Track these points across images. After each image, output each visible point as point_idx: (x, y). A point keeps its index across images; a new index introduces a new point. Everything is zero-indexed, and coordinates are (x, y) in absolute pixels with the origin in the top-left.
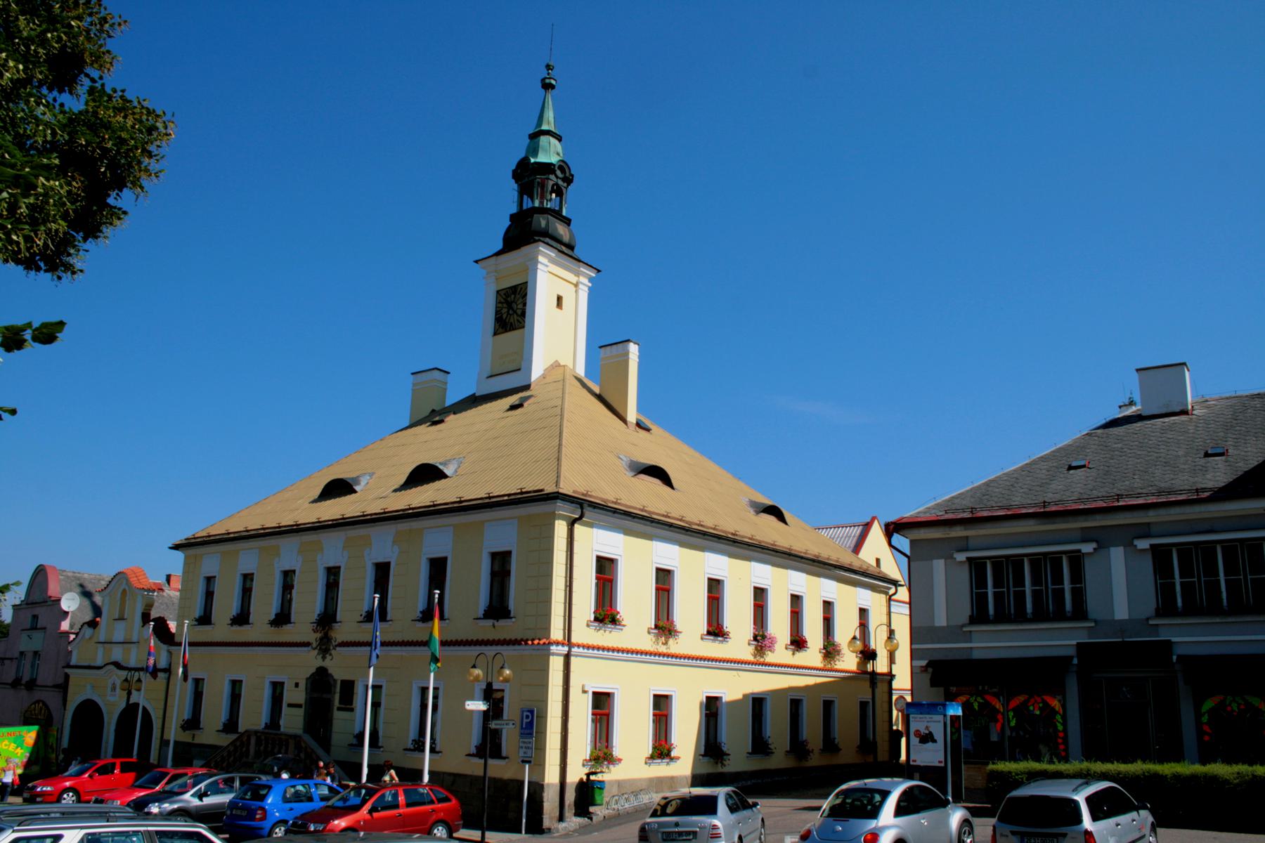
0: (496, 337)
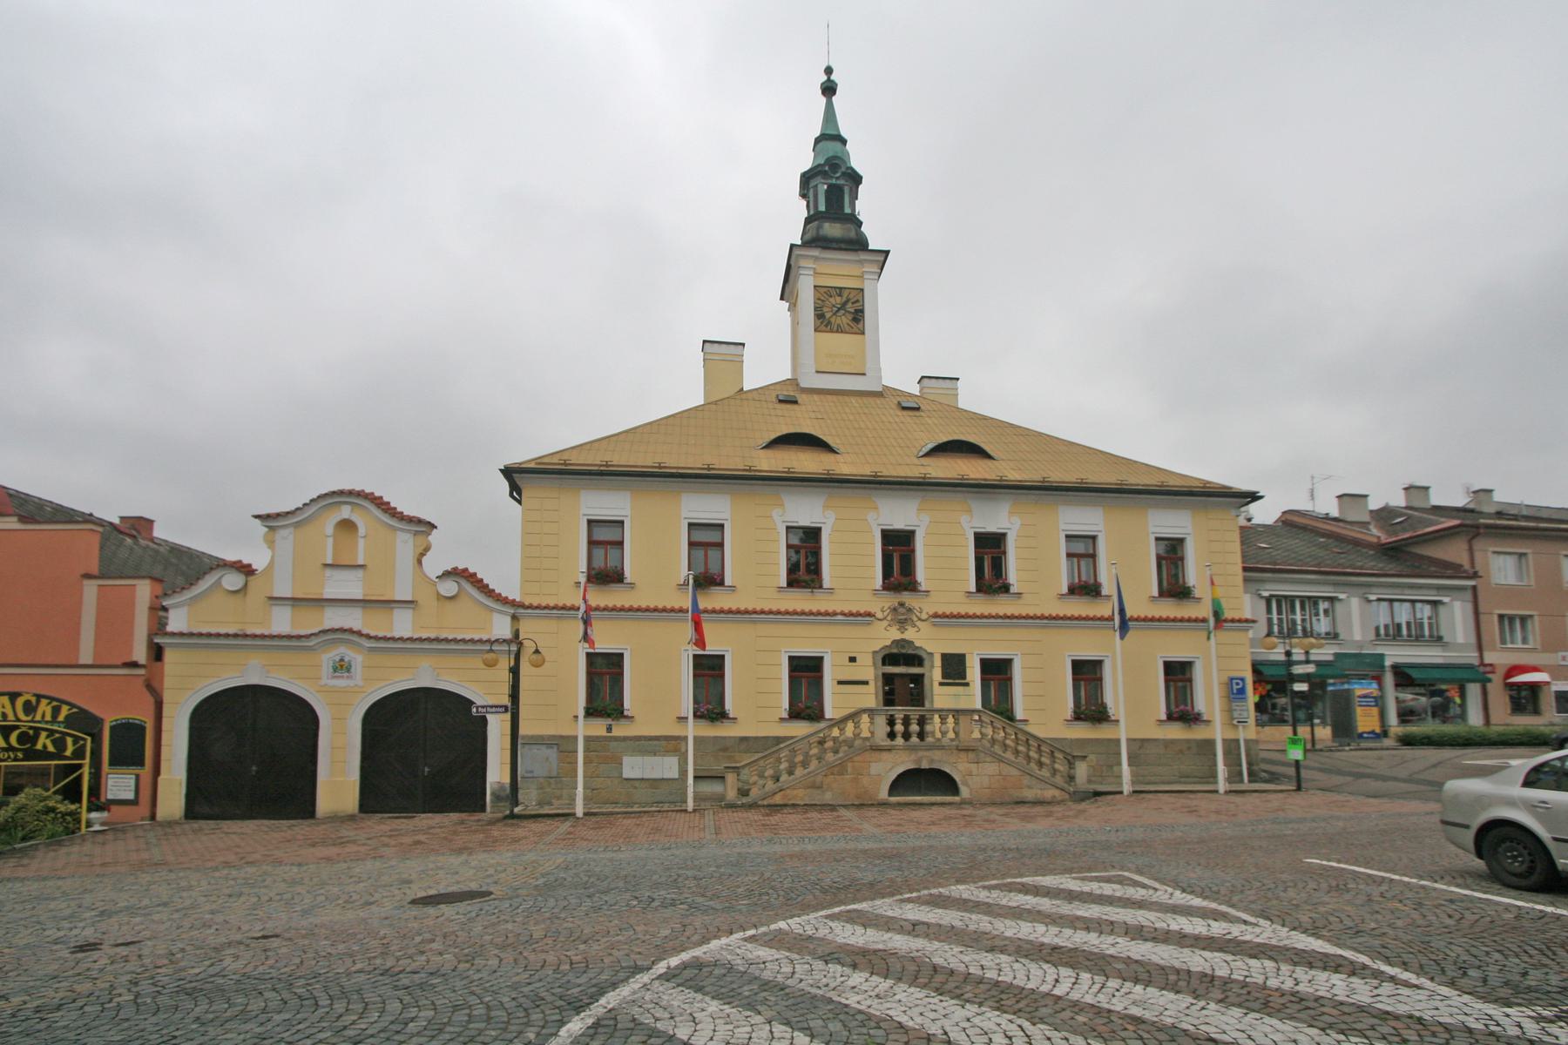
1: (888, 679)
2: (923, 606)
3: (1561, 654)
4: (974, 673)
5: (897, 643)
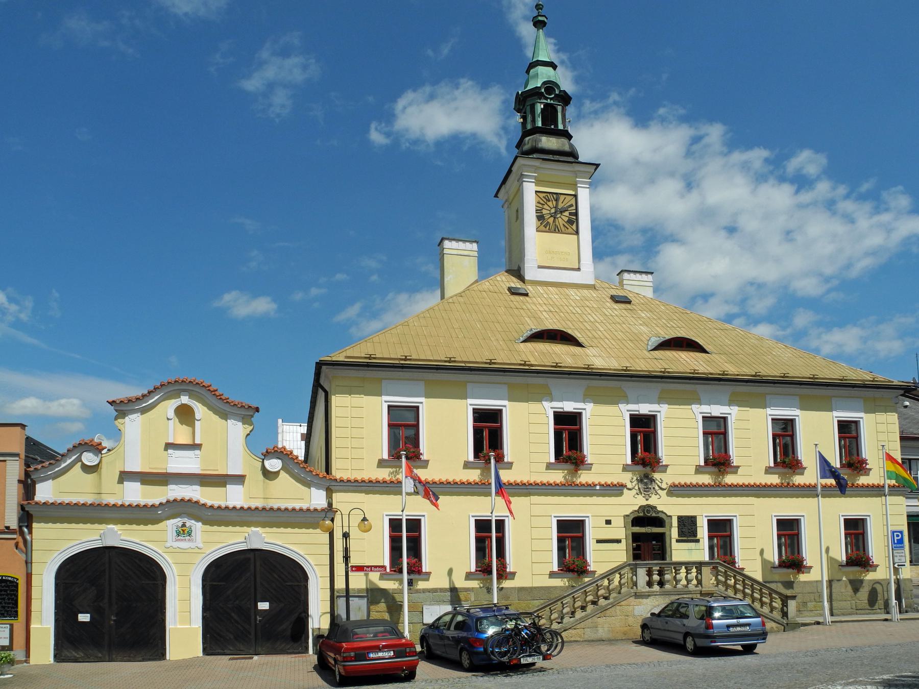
1: (636, 537)
2: (663, 479)
4: (703, 531)
5: (642, 508)
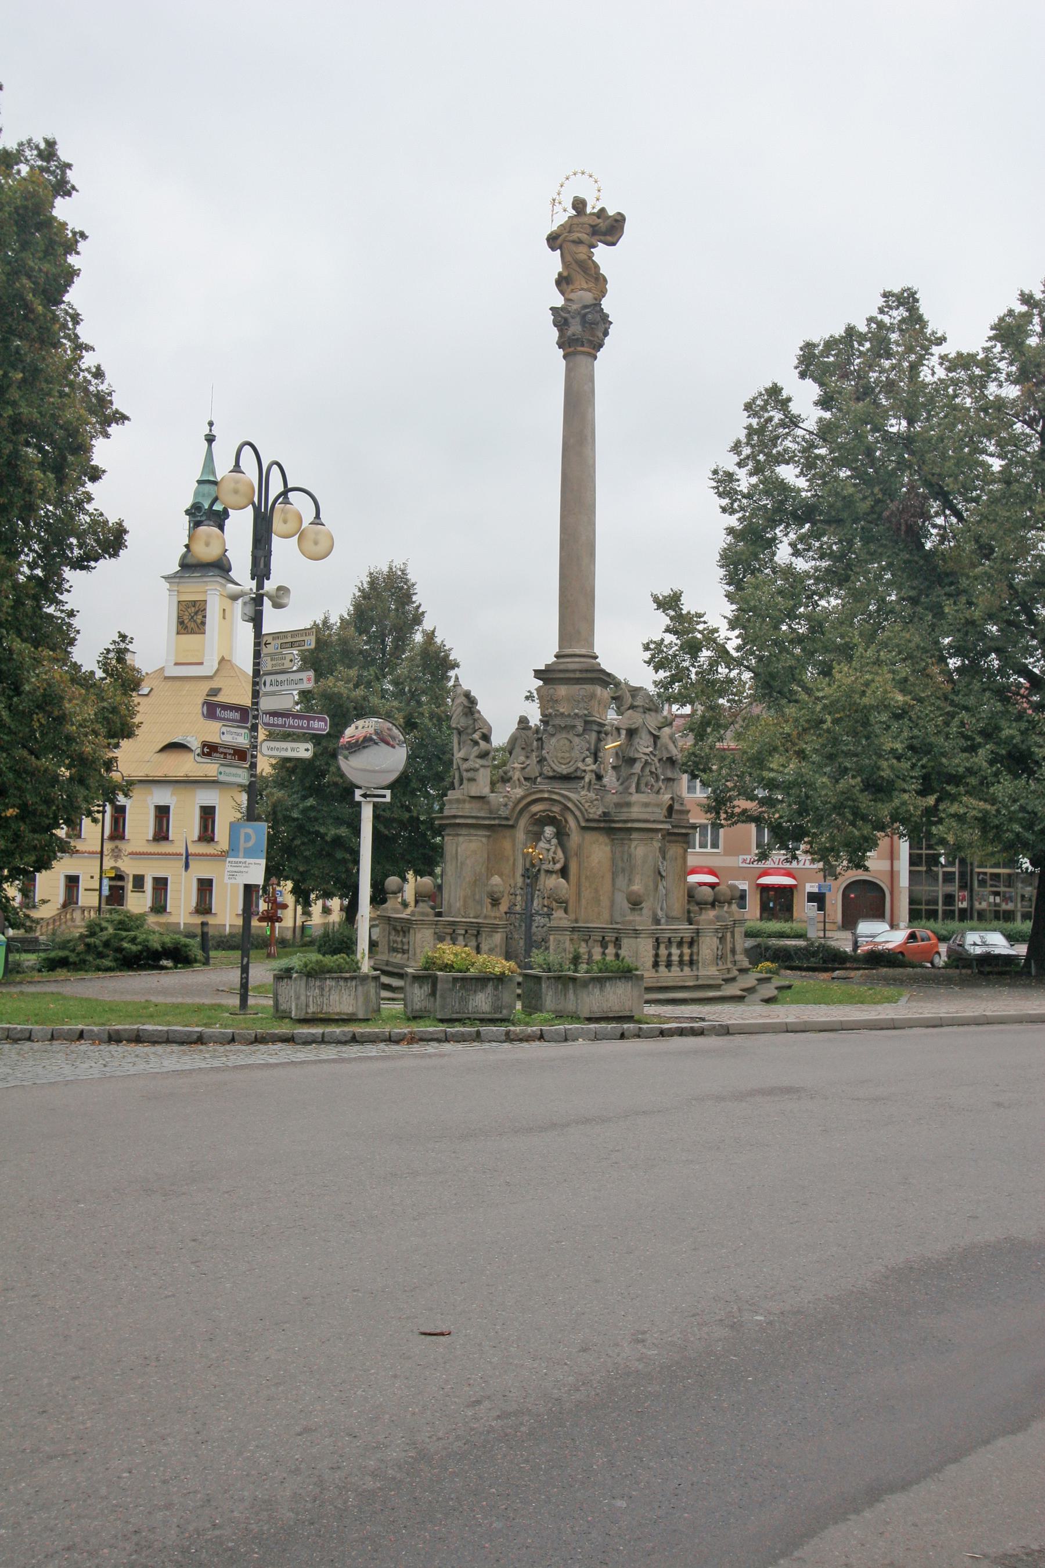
0: (180, 636)
2: (126, 847)
3: (741, 857)
4: (149, 885)
